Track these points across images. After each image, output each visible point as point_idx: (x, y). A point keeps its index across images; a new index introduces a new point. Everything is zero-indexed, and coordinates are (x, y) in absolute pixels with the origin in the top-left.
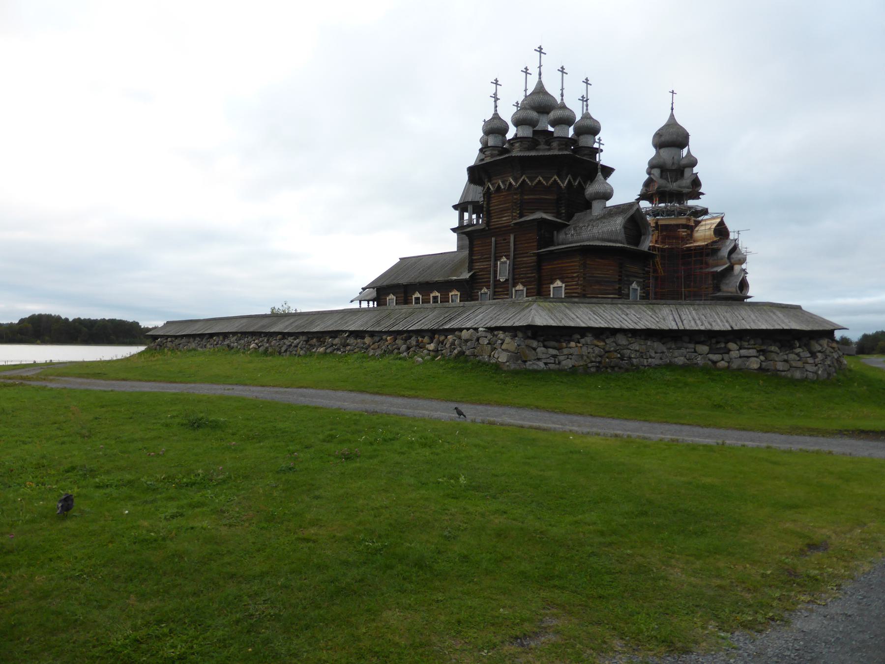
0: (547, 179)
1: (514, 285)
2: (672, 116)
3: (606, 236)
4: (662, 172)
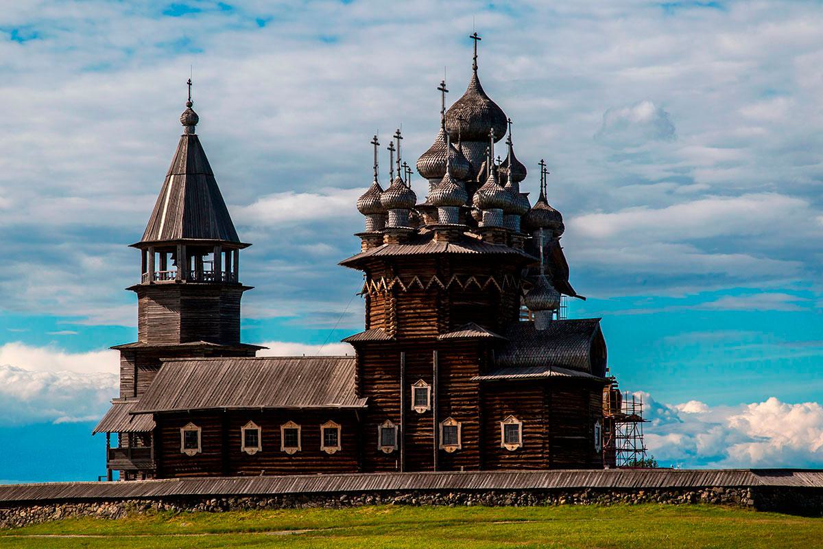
0: (482, 281)
1: (442, 416)
3: (565, 362)
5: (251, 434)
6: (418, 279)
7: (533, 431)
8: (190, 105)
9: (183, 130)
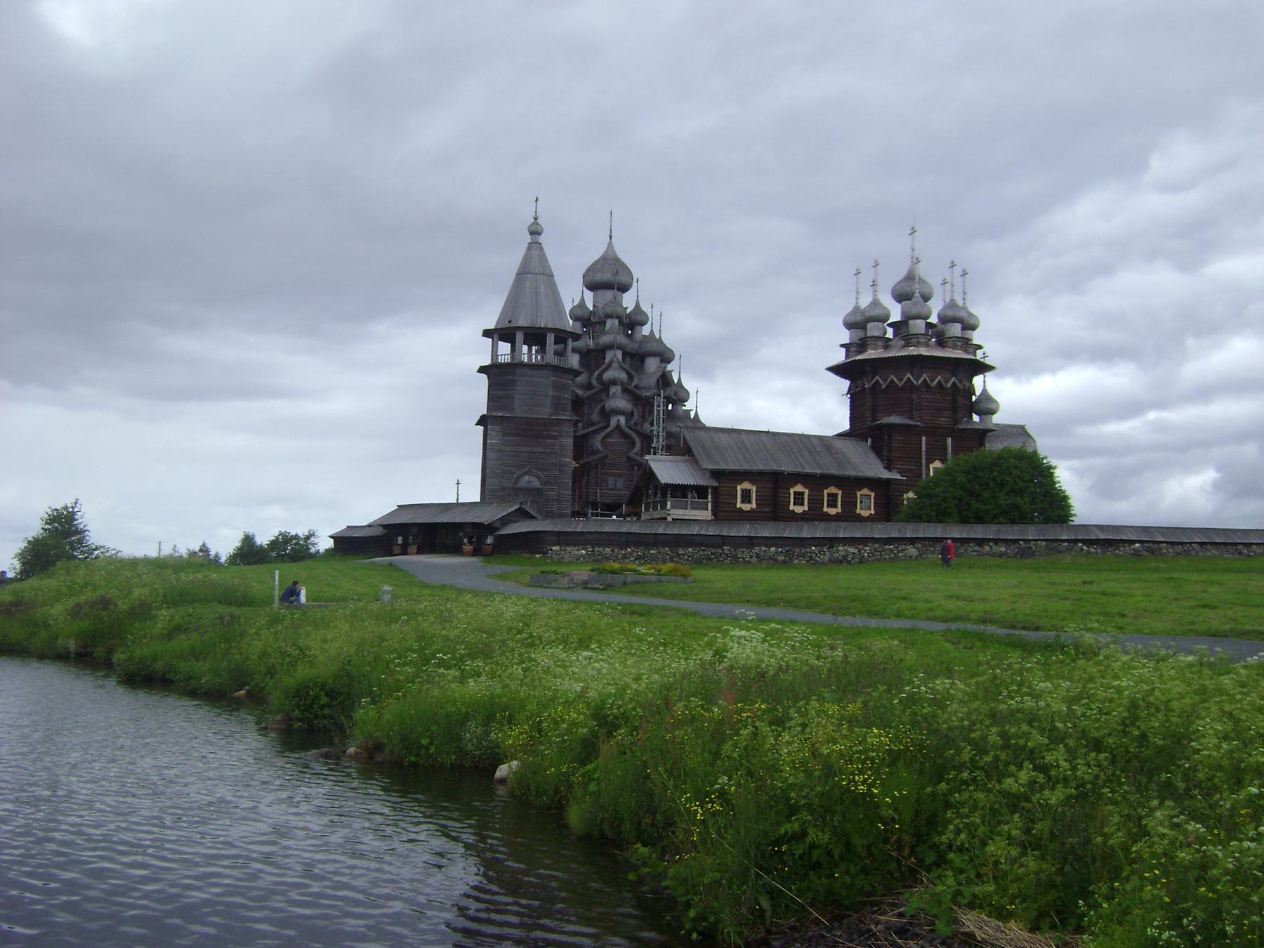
2: (610, 245)
5: (799, 496)
9: (528, 239)
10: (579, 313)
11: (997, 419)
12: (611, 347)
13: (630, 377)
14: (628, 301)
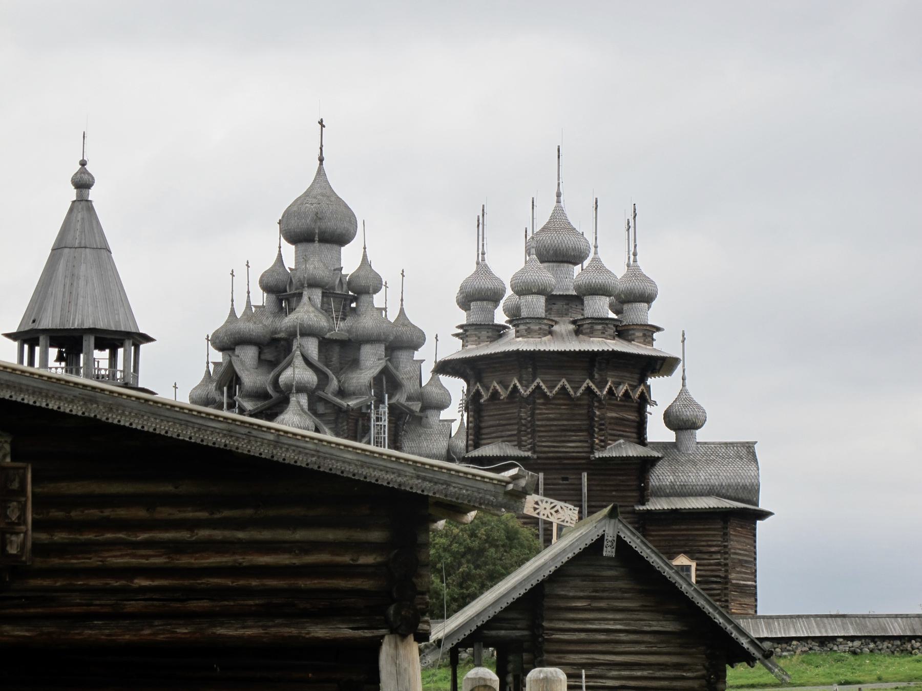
2: (321, 172)
3: (731, 493)
4: (324, 295)
6: (566, 383)
7: (708, 573)
8: (83, 163)
9: (72, 194)
10: (271, 281)
11: (701, 435)
12: (291, 335)
13: (323, 379)
14: (349, 260)
